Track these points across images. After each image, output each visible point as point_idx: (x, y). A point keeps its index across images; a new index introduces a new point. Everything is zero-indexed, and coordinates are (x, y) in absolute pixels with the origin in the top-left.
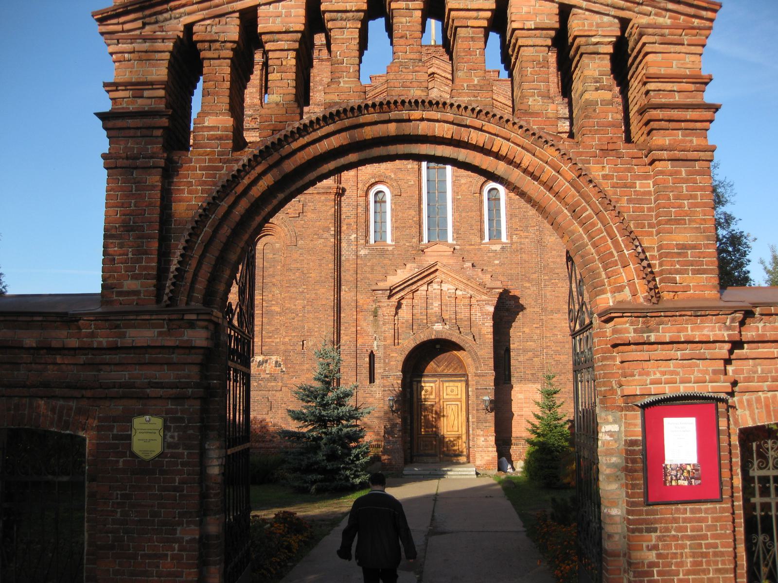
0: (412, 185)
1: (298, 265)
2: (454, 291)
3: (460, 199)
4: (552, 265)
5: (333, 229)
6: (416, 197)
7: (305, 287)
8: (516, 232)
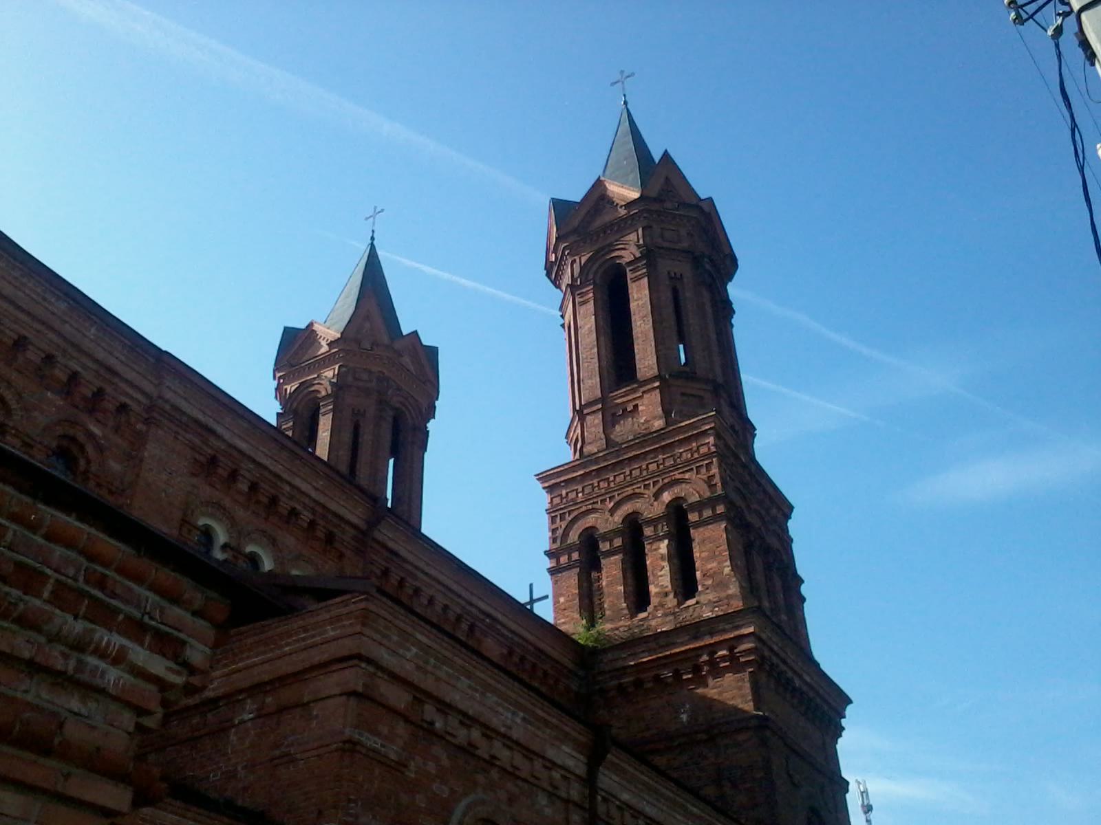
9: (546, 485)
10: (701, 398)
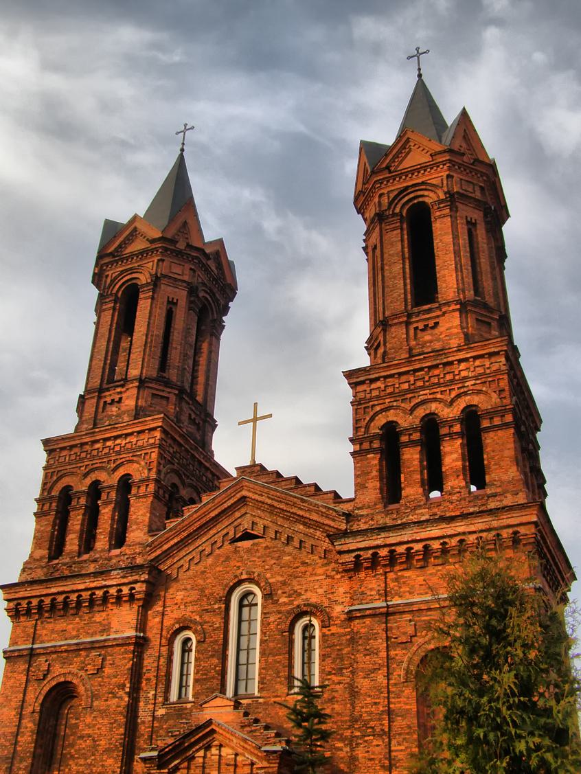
0: (217, 628)
1: (90, 731)
2: (233, 756)
3: (267, 640)
4: (366, 717)
5: (128, 685)
6: (221, 642)
7: (93, 758)
8: (329, 677)
9: (47, 448)
10: (168, 398)
